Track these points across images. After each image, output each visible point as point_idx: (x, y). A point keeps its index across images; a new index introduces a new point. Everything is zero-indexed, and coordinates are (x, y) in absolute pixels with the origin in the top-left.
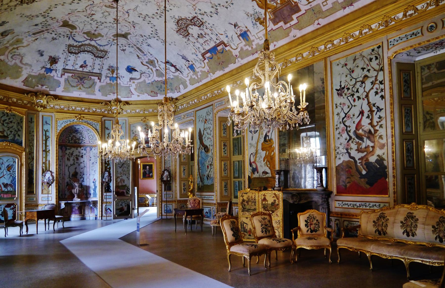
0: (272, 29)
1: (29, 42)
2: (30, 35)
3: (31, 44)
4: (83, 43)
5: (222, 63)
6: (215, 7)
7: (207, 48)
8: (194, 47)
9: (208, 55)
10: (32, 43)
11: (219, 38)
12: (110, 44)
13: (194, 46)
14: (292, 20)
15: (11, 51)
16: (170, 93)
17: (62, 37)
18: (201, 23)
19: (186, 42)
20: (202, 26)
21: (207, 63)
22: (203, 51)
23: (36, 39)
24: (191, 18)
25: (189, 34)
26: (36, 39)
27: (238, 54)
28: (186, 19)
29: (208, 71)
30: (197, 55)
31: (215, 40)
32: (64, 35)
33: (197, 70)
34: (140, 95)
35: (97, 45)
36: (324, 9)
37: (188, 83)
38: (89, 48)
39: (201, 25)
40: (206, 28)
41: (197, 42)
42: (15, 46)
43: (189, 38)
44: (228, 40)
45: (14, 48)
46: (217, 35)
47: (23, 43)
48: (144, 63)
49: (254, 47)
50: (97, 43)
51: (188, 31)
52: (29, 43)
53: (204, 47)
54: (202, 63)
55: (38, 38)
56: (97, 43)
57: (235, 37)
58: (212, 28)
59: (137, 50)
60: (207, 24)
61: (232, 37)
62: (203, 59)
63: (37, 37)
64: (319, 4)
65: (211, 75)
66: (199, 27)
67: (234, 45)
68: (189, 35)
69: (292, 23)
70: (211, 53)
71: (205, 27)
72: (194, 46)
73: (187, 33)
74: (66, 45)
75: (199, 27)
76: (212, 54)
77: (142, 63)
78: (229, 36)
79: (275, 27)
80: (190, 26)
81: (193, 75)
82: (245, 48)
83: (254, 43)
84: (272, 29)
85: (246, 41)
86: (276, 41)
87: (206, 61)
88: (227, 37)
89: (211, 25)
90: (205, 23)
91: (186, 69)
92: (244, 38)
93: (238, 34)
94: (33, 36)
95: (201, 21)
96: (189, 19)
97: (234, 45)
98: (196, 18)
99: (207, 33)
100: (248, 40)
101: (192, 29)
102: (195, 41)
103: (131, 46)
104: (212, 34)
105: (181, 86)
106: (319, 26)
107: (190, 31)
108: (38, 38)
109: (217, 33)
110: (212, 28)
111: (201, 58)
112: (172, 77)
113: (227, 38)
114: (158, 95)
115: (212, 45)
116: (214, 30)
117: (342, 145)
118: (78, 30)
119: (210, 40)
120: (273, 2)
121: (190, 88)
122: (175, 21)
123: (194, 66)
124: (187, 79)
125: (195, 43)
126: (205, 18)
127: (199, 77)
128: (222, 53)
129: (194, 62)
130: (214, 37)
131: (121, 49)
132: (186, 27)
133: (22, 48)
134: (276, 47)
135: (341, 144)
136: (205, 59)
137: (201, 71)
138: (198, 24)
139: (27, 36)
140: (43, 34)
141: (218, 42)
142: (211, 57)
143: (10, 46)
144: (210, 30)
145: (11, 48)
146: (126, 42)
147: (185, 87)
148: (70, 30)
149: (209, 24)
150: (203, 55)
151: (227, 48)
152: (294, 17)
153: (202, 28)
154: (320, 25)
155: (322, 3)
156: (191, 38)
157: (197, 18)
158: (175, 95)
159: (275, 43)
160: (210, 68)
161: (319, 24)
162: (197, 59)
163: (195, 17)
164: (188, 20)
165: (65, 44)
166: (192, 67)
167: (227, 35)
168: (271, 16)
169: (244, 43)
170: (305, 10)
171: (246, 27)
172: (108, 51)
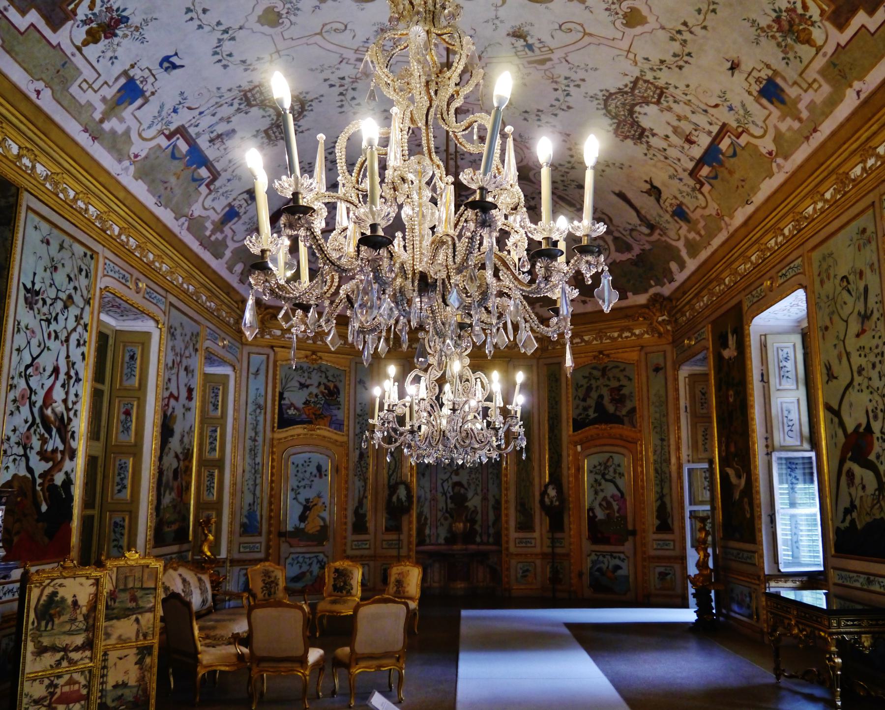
0: (838, 45)
5: (743, 183)
6: (679, 36)
7: (697, 152)
8: (667, 161)
9: (705, 171)
11: (713, 118)
13: (666, 158)
16: (656, 285)
18: (658, 91)
19: (646, 155)
20: (663, 99)
21: (709, 192)
22: (690, 165)
24: (631, 85)
25: (644, 130)
27: (772, 147)
28: (620, 91)
29: (718, 214)
30: (681, 180)
31: (708, 127)
33: (694, 216)
34: (588, 299)
37: (684, 253)
39: (660, 96)
40: (675, 102)
41: (669, 146)
43: (648, 142)
44: (737, 116)
46: (706, 111)
49: (805, 115)
51: (637, 122)
53: (688, 153)
54: (700, 196)
57: (750, 101)
58: (688, 97)
60: (672, 89)
61: (743, 105)
62: (698, 186)
65: (726, 223)
66: (658, 102)
67: (757, 125)
68: (646, 133)
70: (709, 165)
71: (671, 99)
72: (666, 158)
73: (639, 130)
75: (658, 102)
76: (713, 167)
78: (736, 104)
79: (844, 38)
80: (637, 109)
81: (689, 231)
82: (783, 127)
83: (802, 106)
84: (838, 45)
85: (781, 106)
86: (861, 78)
87: (706, 188)
88: (731, 108)
89: (682, 86)
90: (667, 89)
91: (670, 219)
92: (774, 100)
93: (755, 94)
95: (657, 87)
96: (627, 89)
97: (757, 125)
98: (641, 82)
99: (682, 114)
100: (783, 102)
101: (645, 114)
102: (664, 144)
104: (693, 113)
105: (674, 266)
107: (645, 123)
109: (705, 107)
110: (688, 97)
111: (692, 182)
112: (647, 247)
113: (732, 112)
114: (630, 294)
115: (704, 141)
116: (694, 100)
117: (17, 432)
119: (696, 130)
121: (692, 265)
122: (599, 107)
123: (684, 207)
124: (680, 244)
125: (665, 150)
126: (664, 77)
127: (703, 232)
128: (735, 154)
129: (681, 199)
130: (701, 120)
132: (631, 112)
134: (863, 96)
135: (14, 430)
136: (702, 184)
137: (702, 216)
138: (653, 97)
141: (715, 129)
142: (712, 175)
144: (685, 103)
147: (682, 265)
149: (676, 88)
150: (693, 173)
151: (743, 140)
153: (665, 104)
156: (653, 141)
157: (646, 81)
158: (667, 290)
159: (857, 85)
160: (719, 205)
162: (685, 189)
163: (637, 79)
164: (626, 93)
166: (680, 213)
167: (729, 104)
168: (827, 9)
169: (776, 113)
171: (768, 66)
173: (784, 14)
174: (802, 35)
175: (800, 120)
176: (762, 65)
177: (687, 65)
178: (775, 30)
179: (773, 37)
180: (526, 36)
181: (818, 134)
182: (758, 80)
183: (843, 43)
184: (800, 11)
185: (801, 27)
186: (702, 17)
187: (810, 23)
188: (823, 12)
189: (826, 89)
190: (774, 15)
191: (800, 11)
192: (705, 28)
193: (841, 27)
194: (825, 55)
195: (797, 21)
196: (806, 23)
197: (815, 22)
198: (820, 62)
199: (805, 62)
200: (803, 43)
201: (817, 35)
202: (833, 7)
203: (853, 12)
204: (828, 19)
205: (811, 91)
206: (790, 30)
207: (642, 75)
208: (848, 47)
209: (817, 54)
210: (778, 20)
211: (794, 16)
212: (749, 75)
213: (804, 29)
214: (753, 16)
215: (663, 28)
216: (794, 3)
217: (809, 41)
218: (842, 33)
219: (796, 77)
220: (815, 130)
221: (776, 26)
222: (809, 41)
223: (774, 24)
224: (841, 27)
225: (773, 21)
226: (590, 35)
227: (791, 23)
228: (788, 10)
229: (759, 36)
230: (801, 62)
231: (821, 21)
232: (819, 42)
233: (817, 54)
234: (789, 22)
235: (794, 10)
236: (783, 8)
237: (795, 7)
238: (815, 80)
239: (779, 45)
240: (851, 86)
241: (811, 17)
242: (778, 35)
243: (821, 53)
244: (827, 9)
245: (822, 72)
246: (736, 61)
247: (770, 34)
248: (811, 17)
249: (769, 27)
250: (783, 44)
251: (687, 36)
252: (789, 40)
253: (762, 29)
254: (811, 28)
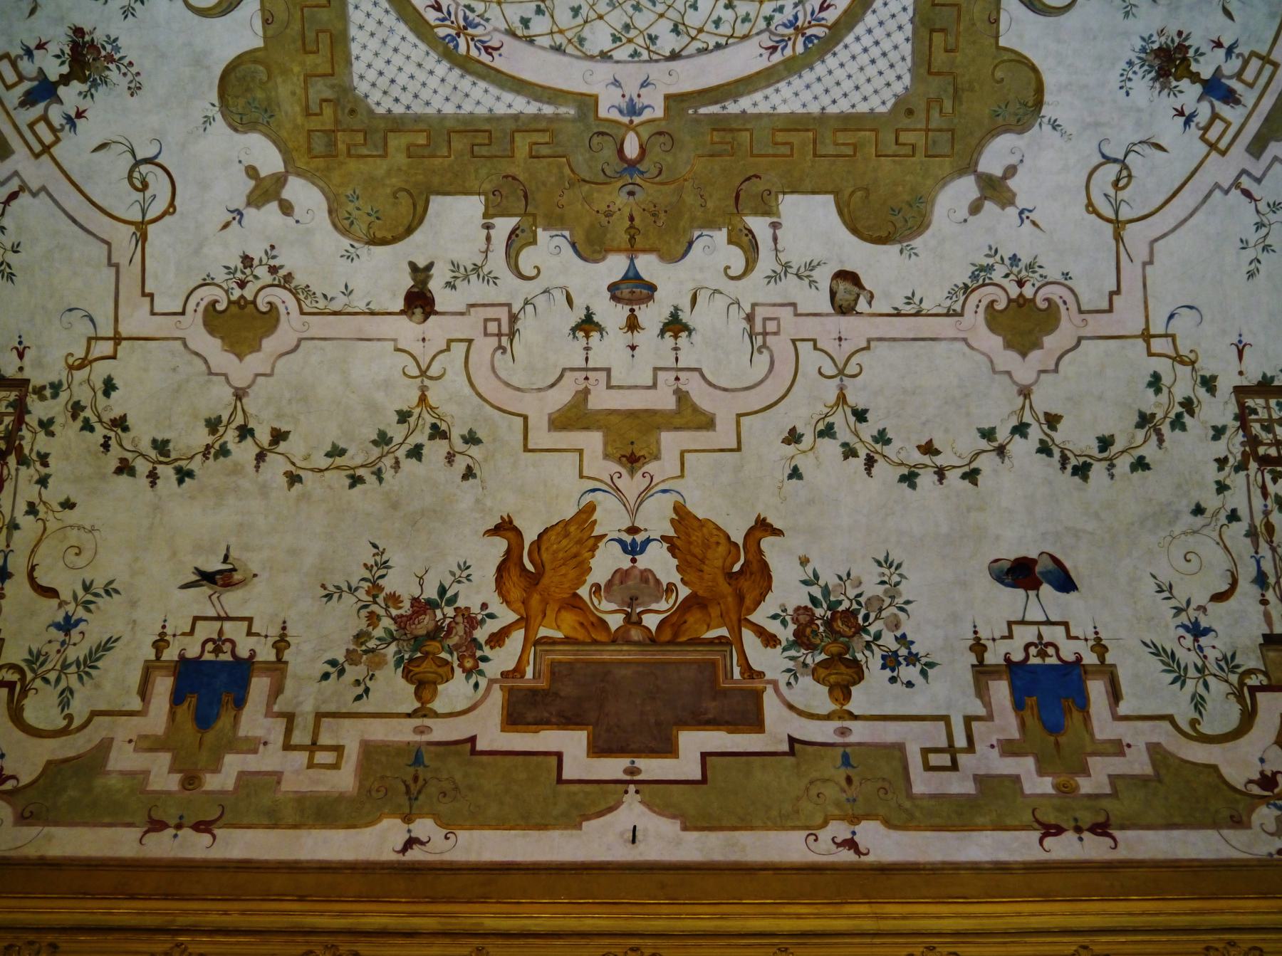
0: (473, 740)
14: (669, 749)
36: (922, 783)
64: (900, 748)
69: (652, 768)
78: (94, 630)
79: (493, 737)
83: (233, 764)
84: (473, 740)
86: (449, 824)
93: (170, 654)
106: (847, 856)
120: (606, 605)
152: (693, 742)
154: (858, 852)
155: (925, 752)
159: (424, 827)
161: (851, 844)
168: (529, 673)
170: (792, 741)
171: (281, 643)
173: (450, 611)
174: (427, 666)
175: (191, 781)
176: (274, 632)
177: (146, 482)
178: (394, 612)
179: (373, 619)
180: (83, 80)
181: (206, 838)
182: (219, 643)
183: (481, 746)
184: (481, 634)
185: (444, 655)
186: (324, 462)
187: (469, 664)
188: (518, 671)
189: (345, 780)
190: (431, 593)
191: (481, 634)
192: (293, 479)
193: (513, 719)
194: (419, 730)
195: (454, 640)
196: (461, 658)
197: (481, 673)
198: (402, 732)
199: (362, 707)
200: (407, 675)
201: (455, 692)
202: (543, 684)
203: (568, 721)
204: (510, 693)
205: (302, 757)
206: (418, 642)
207: (39, 391)
208: (484, 758)
209: (409, 715)
210: (422, 607)
211: (460, 629)
212: (219, 618)
213: (447, 663)
214: (396, 557)
215: (239, 395)
216: (491, 616)
217: (424, 687)
218: (503, 730)
219: (308, 707)
220: (203, 826)
221: (406, 608)
222: (424, 687)
223: (407, 605)
224: (513, 719)
225: (415, 600)
226: (142, 238)
227: (436, 633)
228: (465, 613)
229: (352, 590)
230: (359, 698)
231: (492, 681)
232: (438, 705)
233: (409, 715)
234: (438, 628)
235: (473, 622)
236: (461, 603)
237: (482, 622)
238: (339, 749)
239: (360, 637)
240: (408, 819)
241: (485, 659)
242: (386, 622)
243: (417, 722)
244: (529, 673)
245: (369, 750)
246: (237, 576)
247: (374, 608)
248: (485, 659)
249: (394, 599)
250: (372, 644)
251: (244, 452)
252: (393, 648)
253: (375, 590)
254: (458, 671)
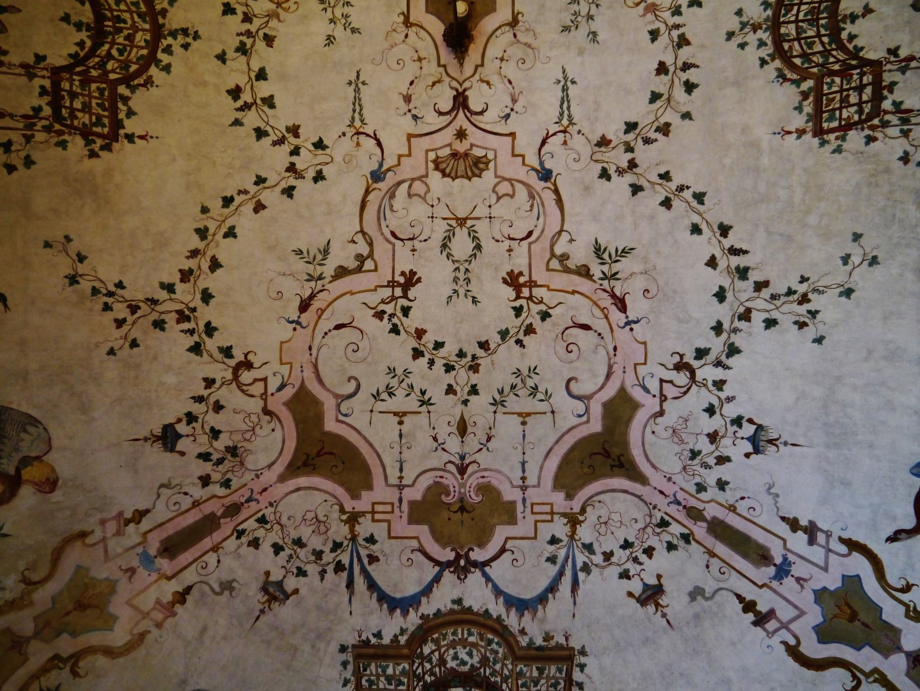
1: (146, 615)
2: (147, 560)
3: (155, 632)
4: (428, 607)
10: (159, 625)
12: (567, 579)
15: (35, 676)
17: (313, 569)
23: (181, 597)
26: (181, 597)
32: (318, 555)
35: (497, 608)
38: (464, 643)
42: (65, 645)
45: (56, 661)
47: (109, 622)
48: (813, 648)
50: (498, 592)
52: (143, 626)
55: (188, 590)
56: (498, 592)
59: (721, 549)
63: (190, 576)
74: (343, 649)
77: (794, 652)
94: (164, 564)
103: (676, 529)
108: (188, 590)
118: (380, 492)
131: (636, 586)
133: (101, 661)
139: (135, 563)
140: (215, 549)
143: (36, 635)
145: (38, 654)
146: (637, 512)
148: (340, 491)
165: (334, 647)
172: (575, 644)
